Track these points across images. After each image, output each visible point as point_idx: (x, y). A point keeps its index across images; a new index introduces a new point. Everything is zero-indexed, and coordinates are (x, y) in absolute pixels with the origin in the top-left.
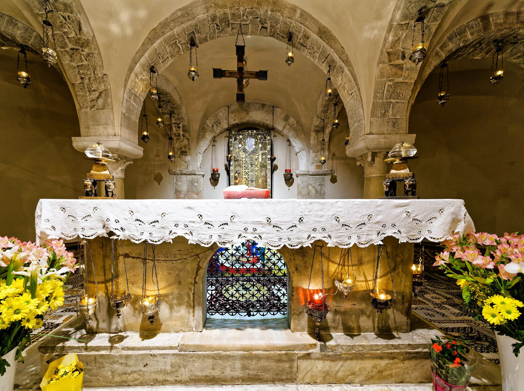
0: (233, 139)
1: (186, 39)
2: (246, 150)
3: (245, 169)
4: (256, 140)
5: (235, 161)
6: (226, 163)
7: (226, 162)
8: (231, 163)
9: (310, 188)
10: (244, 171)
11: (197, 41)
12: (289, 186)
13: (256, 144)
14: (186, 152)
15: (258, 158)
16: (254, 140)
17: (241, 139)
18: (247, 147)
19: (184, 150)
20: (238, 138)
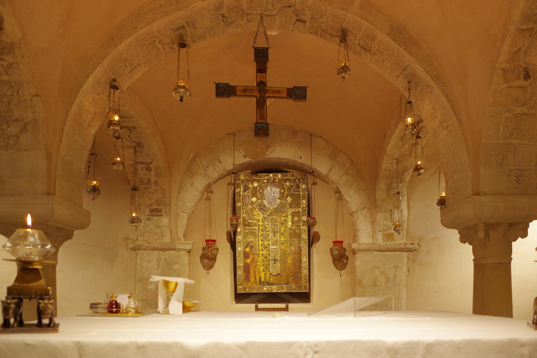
0: (242, 188)
1: (172, 36)
2: (265, 206)
3: (262, 240)
4: (282, 191)
5: (245, 225)
6: (229, 229)
7: (230, 228)
8: (239, 230)
10: (261, 243)
11: (188, 40)
12: (339, 270)
13: (282, 196)
14: (161, 211)
15: (286, 220)
16: (278, 190)
17: (255, 188)
18: (266, 203)
19: (155, 207)
20: (250, 186)
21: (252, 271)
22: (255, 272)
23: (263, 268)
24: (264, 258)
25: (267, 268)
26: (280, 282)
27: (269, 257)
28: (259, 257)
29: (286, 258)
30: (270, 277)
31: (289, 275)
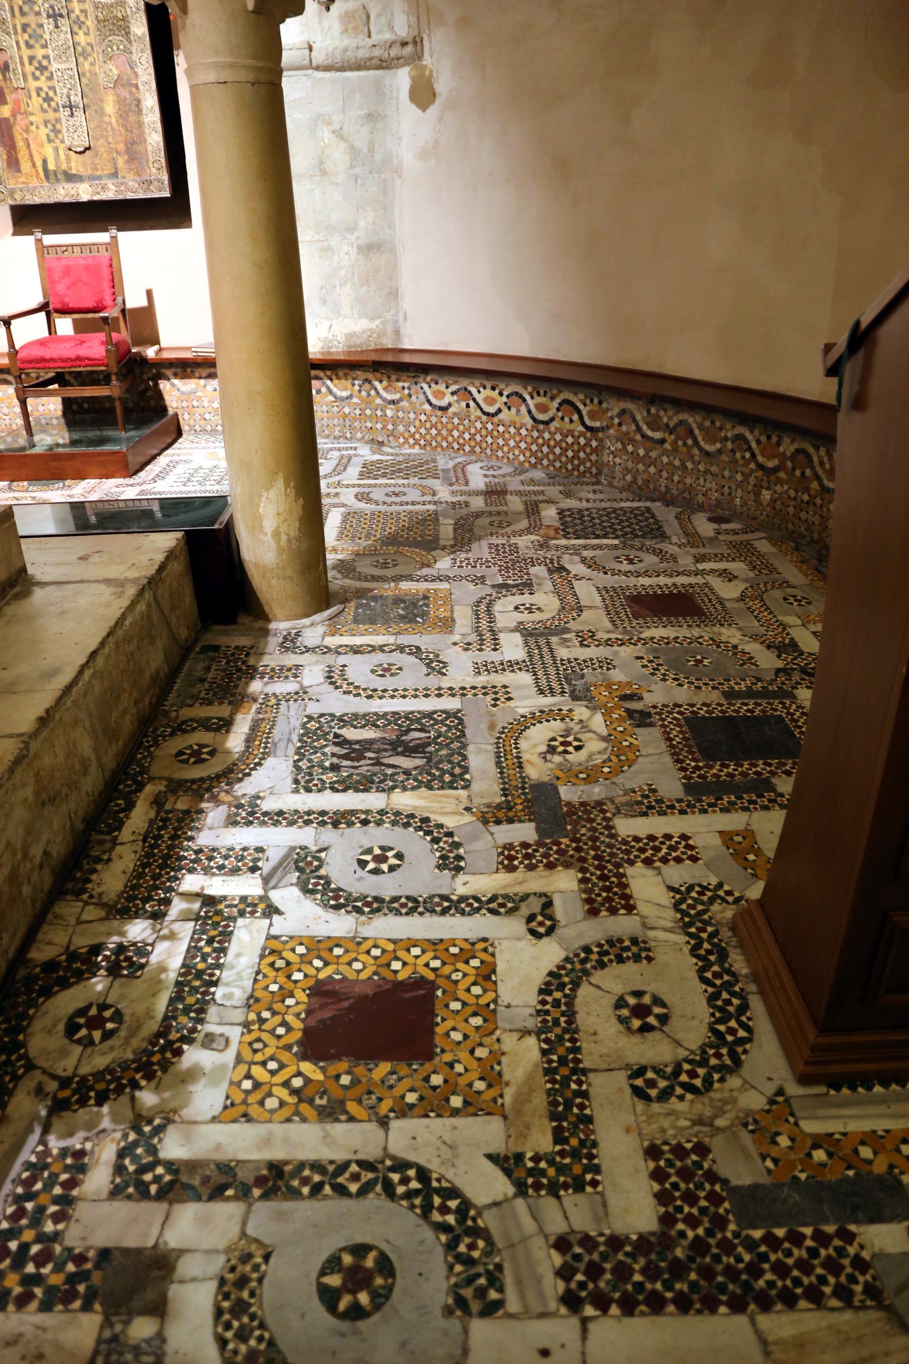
3: (29, 46)
9: (326, 135)
10: (26, 53)
21: (20, 144)
22: (28, 146)
23: (47, 131)
24: (44, 100)
25: (56, 132)
26: (97, 170)
27: (55, 98)
28: (30, 97)
29: (102, 100)
30: (68, 159)
31: (117, 152)
